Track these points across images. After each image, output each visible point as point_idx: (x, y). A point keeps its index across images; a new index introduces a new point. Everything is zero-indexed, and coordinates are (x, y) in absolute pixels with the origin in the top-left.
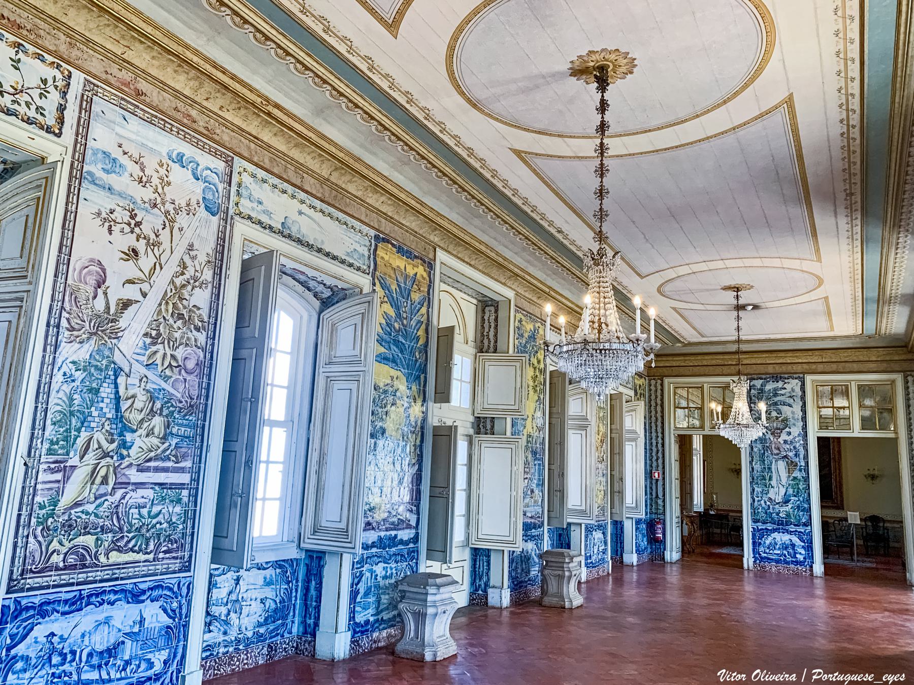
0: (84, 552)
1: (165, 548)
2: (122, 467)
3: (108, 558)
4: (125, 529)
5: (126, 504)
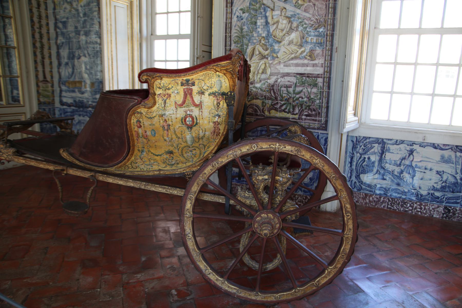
0: (256, 108)
1: (306, 113)
2: (274, 63)
3: (270, 113)
4: (279, 99)
5: (279, 85)
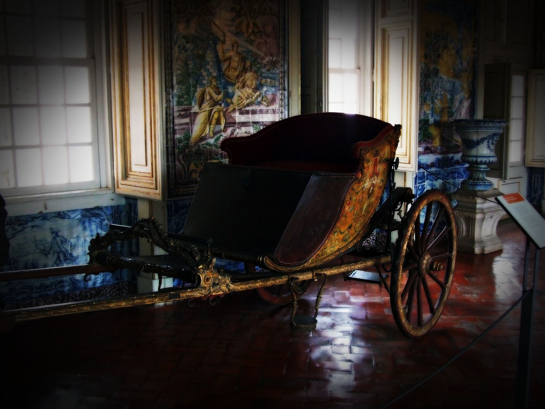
2: (229, 111)
